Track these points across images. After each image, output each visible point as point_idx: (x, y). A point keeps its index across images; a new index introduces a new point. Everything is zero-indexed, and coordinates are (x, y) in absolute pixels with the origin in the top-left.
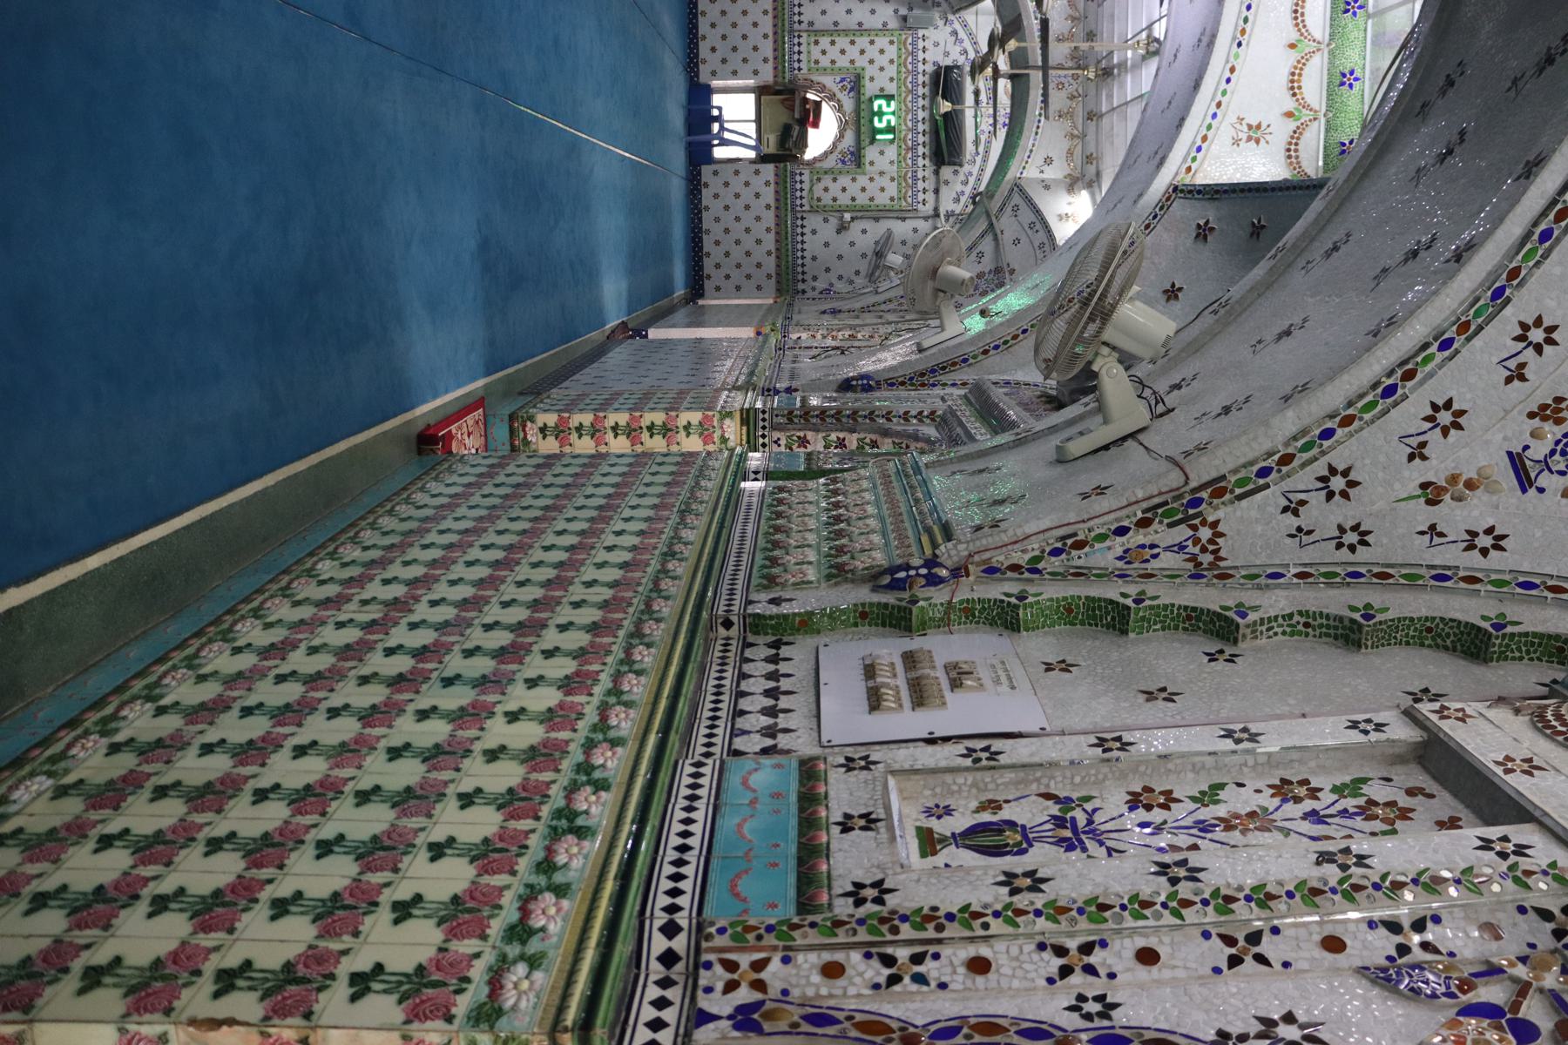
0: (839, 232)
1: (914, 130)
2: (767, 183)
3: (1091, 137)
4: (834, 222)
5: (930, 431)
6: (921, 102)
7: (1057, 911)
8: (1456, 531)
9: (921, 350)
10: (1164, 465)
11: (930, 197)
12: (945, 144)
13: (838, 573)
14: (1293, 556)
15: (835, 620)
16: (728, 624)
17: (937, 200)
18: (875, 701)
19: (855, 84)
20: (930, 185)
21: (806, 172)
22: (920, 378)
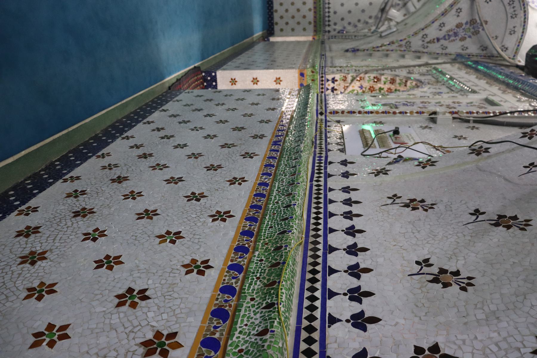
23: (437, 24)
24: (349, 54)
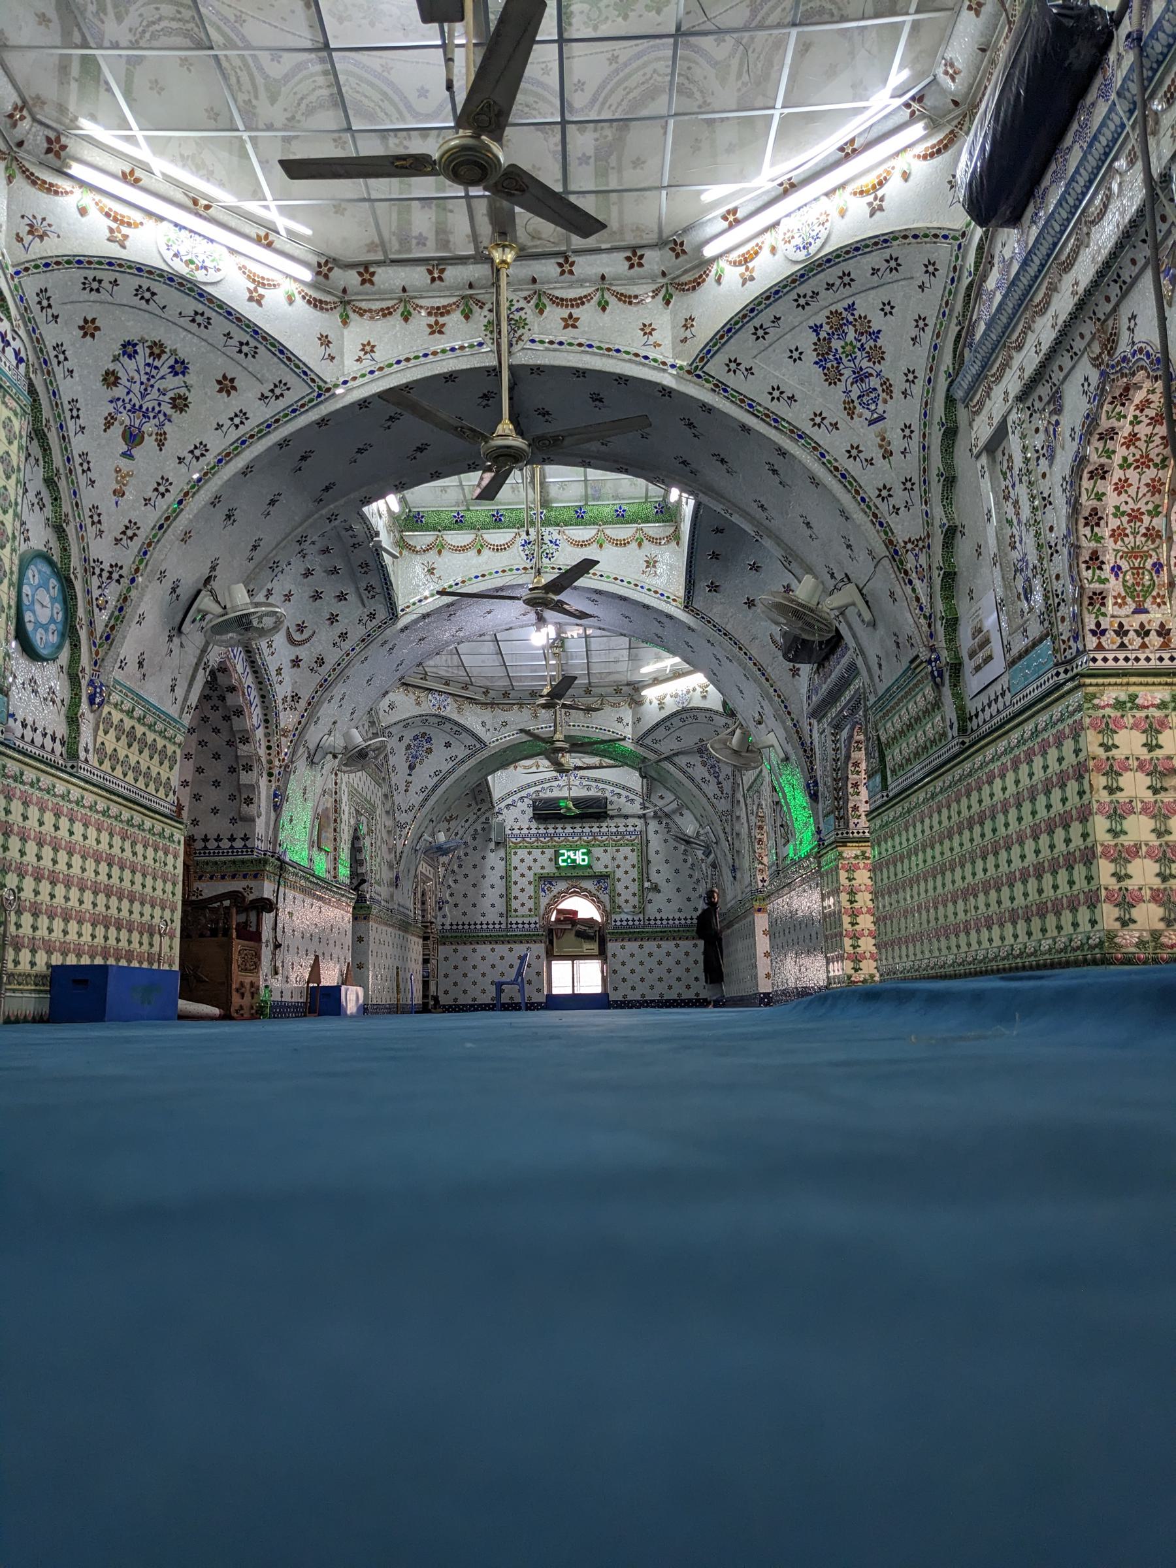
0: (659, 891)
1: (580, 835)
2: (623, 947)
3: (602, 691)
4: (651, 895)
5: (844, 734)
6: (559, 830)
7: (1041, 559)
8: (904, 443)
9: (787, 759)
10: (880, 567)
11: (631, 821)
12: (592, 811)
13: (937, 705)
14: (919, 508)
15: (958, 696)
16: (963, 743)
17: (633, 816)
18: (989, 658)
19: (545, 880)
20: (621, 822)
21: (614, 917)
22: (808, 752)
23: (703, 786)
24: (738, 875)
